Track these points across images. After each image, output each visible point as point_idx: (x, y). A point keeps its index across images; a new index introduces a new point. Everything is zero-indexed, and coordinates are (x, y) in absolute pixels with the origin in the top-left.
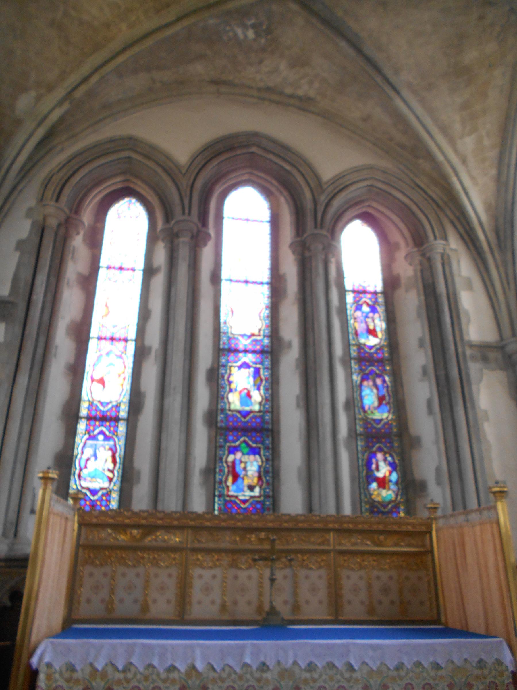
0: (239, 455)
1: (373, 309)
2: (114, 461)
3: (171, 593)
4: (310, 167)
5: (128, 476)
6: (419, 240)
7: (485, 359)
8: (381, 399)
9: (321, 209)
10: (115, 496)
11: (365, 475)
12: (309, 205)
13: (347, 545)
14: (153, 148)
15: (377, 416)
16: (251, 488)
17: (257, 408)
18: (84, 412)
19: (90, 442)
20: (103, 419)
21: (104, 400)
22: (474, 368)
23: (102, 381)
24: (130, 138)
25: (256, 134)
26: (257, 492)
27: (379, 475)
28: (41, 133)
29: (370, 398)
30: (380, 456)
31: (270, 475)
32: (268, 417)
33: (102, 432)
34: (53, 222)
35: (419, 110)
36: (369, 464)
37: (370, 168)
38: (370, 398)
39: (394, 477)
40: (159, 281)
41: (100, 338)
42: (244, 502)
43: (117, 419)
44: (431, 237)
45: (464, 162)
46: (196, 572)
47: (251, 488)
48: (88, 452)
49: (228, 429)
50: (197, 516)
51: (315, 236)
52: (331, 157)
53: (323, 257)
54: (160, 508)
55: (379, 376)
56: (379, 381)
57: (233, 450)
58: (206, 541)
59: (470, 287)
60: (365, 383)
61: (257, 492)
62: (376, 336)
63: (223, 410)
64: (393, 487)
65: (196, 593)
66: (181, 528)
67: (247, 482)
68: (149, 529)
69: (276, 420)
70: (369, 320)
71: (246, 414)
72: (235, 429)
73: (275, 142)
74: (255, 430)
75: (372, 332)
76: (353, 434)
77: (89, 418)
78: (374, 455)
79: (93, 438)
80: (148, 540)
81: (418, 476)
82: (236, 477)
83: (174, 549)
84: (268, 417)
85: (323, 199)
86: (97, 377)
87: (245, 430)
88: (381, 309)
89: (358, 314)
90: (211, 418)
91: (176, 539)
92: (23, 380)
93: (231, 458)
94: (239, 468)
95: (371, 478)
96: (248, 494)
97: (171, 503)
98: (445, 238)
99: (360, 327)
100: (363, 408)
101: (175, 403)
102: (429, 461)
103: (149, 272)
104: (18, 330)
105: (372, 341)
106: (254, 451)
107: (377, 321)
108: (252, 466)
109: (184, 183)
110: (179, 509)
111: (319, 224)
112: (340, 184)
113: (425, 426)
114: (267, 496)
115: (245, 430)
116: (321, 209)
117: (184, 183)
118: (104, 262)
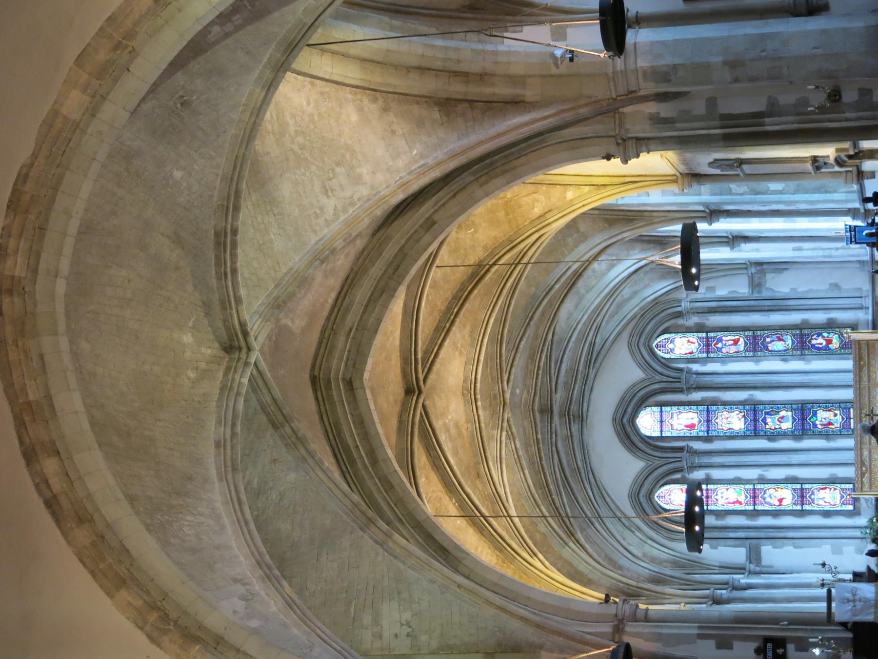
0: (817, 422)
1: (720, 340)
2: (825, 488)
4: (634, 385)
5: (833, 481)
6: (679, 315)
7: (759, 285)
8: (780, 339)
9: (665, 379)
10: (843, 486)
11: (825, 352)
13: (865, 379)
14: (635, 482)
15: (789, 342)
16: (835, 415)
17: (790, 413)
18: (799, 508)
19: (816, 502)
20: (802, 497)
21: (791, 497)
22: (765, 294)
23: (781, 500)
24: (630, 497)
25: (614, 420)
26: (837, 412)
27: (824, 343)
28: (650, 542)
29: (778, 346)
30: (813, 342)
31: (828, 405)
32: (795, 406)
33: (810, 497)
35: (612, 325)
36: (818, 349)
37: (630, 345)
38: (778, 346)
39: (825, 334)
41: (755, 504)
42: (843, 419)
43: (802, 489)
44: (679, 309)
45: (635, 293)
47: (835, 415)
48: (821, 502)
49: (803, 429)
50: (856, 444)
51: (687, 382)
53: (694, 376)
54: (853, 462)
55: (765, 340)
56: (768, 340)
57: (815, 426)
59: (711, 289)
60: (770, 348)
61: (837, 412)
62: (738, 340)
63: (792, 432)
64: (831, 335)
66: (861, 449)
67: (832, 417)
68: (862, 463)
69: (797, 402)
70: (728, 343)
71: (794, 419)
72: (803, 425)
74: (803, 414)
75: (736, 342)
76: (802, 357)
77: (802, 504)
78: (813, 346)
79: (813, 500)
80: (867, 463)
81: (825, 321)
82: (830, 424)
83: (870, 452)
84: (795, 406)
85: (658, 377)
86: (777, 503)
87: (803, 419)
89: (724, 350)
92: (791, 534)
93: (819, 426)
94: (825, 422)
95: (827, 348)
96: (839, 418)
97: (850, 456)
98: (680, 301)
99: (733, 349)
100: (785, 350)
101: (795, 458)
102: (819, 317)
104: (764, 541)
106: (815, 414)
107: (728, 338)
108: (823, 416)
109: (658, 462)
110: (853, 452)
111: (678, 380)
112: (645, 366)
113: (795, 318)
114: (840, 407)
115: (803, 419)
116: (665, 379)
117: (658, 462)
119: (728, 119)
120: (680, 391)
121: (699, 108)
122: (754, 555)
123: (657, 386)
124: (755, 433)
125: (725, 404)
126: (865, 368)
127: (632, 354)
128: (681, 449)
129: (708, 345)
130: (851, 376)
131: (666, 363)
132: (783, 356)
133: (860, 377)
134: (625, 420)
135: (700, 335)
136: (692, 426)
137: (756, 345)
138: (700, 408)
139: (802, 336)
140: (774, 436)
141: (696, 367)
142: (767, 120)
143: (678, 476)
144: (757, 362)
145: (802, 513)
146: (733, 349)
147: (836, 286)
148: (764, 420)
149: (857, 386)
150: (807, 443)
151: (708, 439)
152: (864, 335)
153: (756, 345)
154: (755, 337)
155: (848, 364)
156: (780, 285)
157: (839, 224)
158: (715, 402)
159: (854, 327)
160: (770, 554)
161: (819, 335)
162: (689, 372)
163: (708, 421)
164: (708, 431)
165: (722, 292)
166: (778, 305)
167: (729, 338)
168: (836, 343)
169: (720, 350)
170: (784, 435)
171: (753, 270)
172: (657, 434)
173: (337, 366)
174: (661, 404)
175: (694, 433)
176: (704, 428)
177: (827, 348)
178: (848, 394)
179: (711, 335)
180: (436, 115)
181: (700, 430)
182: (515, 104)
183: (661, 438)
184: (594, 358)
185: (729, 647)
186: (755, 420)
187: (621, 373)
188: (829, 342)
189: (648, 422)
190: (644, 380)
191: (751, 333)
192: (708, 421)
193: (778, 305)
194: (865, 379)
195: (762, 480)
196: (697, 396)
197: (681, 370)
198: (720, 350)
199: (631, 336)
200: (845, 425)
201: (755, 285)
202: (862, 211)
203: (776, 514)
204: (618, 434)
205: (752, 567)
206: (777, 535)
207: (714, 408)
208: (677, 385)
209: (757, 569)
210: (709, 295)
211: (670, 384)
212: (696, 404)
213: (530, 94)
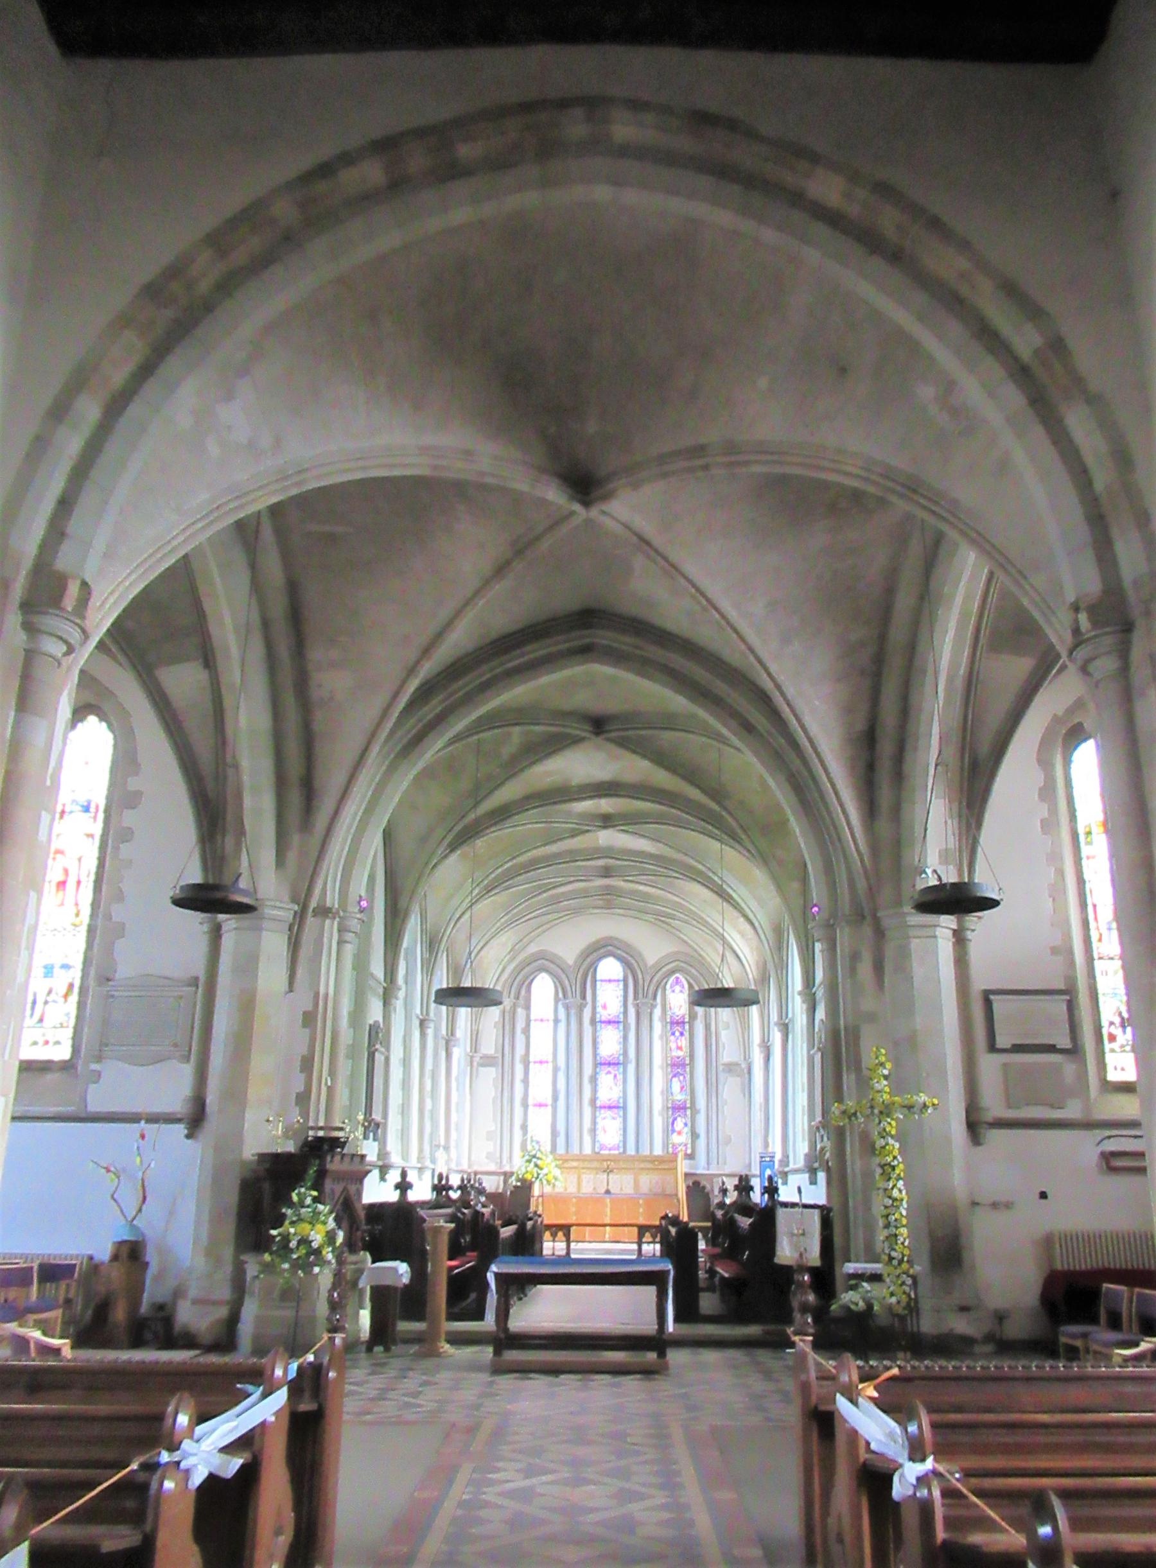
1: (682, 1034)
3: (575, 1184)
7: (730, 1071)
8: (682, 1088)
11: (669, 1129)
12: (641, 982)
13: (642, 1165)
22: (722, 1076)
25: (611, 938)
30: (679, 1119)
34: (508, 1008)
36: (673, 1124)
38: (676, 1085)
40: (562, 1026)
46: (584, 1176)
52: (653, 947)
58: (586, 1164)
65: (584, 1183)
68: (566, 1161)
73: (620, 941)
75: (680, 1048)
78: (675, 1119)
80: (566, 1165)
83: (575, 1168)
85: (648, 978)
88: (687, 1034)
89: (672, 1038)
90: (593, 1101)
91: (575, 1164)
92: (506, 1094)
95: (673, 1131)
103: (556, 1021)
105: (680, 1053)
109: (572, 977)
113: (701, 1103)
118: (532, 1017)
119: (854, 1035)
120: (636, 998)
121: (868, 1004)
122: (488, 1061)
123: (640, 976)
124: (599, 1064)
125: (625, 1038)
126: (650, 1166)
127: (668, 955)
128: (584, 997)
129: (678, 1023)
130: (647, 1153)
131: (661, 985)
132: (667, 1091)
133: (643, 1161)
134: (610, 948)
135: (687, 1017)
136: (604, 1007)
137: (677, 1067)
138: (621, 1016)
139: (685, 1108)
140: (594, 1079)
141: (657, 1012)
142: (853, 1076)
143: (561, 995)
144: (662, 1068)
145: (525, 1105)
146: (673, 1046)
147: (728, 1141)
148: (609, 1072)
149: (632, 1159)
150: (587, 1110)
151: (593, 1022)
152: (683, 1166)
153: (677, 1067)
154: (684, 1065)
155: (658, 1151)
156: (730, 1087)
157: (776, 1148)
158: (626, 1029)
159: (691, 1157)
160: (489, 1074)
161: (686, 1125)
162: (653, 1007)
163: (609, 1022)
164: (601, 1022)
165: (724, 1034)
166: (713, 1087)
167: (684, 1042)
168: (676, 1139)
169: (673, 1034)
170: (595, 1091)
171: (744, 1066)
172: (598, 977)
173: (604, 637)
174: (625, 980)
175: (599, 1009)
176: (603, 1019)
177: (673, 1131)
178: (631, 1151)
179: (687, 1027)
180: (860, 726)
181: (603, 1014)
182: (870, 809)
183: (594, 981)
184: (662, 919)
185: (305, 1025)
186: (609, 1064)
187: (653, 947)
188: (679, 1133)
189: (610, 968)
190: (646, 965)
191: (687, 1062)
192: (609, 1022)
193: (713, 1087)
194: (642, 1165)
195: (556, 1070)
196: (632, 1011)
197: (655, 998)
198: (673, 1034)
199: (687, 954)
200: (602, 1147)
201: (731, 1068)
202: (786, 1169)
203: (526, 1081)
204: (598, 941)
205: (477, 1059)
206: (505, 1083)
207: (621, 1027)
208: (641, 996)
209: (475, 1064)
210: (720, 1025)
211: (643, 986)
212: (625, 1012)
213: (884, 826)
